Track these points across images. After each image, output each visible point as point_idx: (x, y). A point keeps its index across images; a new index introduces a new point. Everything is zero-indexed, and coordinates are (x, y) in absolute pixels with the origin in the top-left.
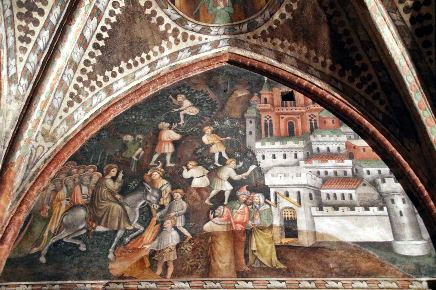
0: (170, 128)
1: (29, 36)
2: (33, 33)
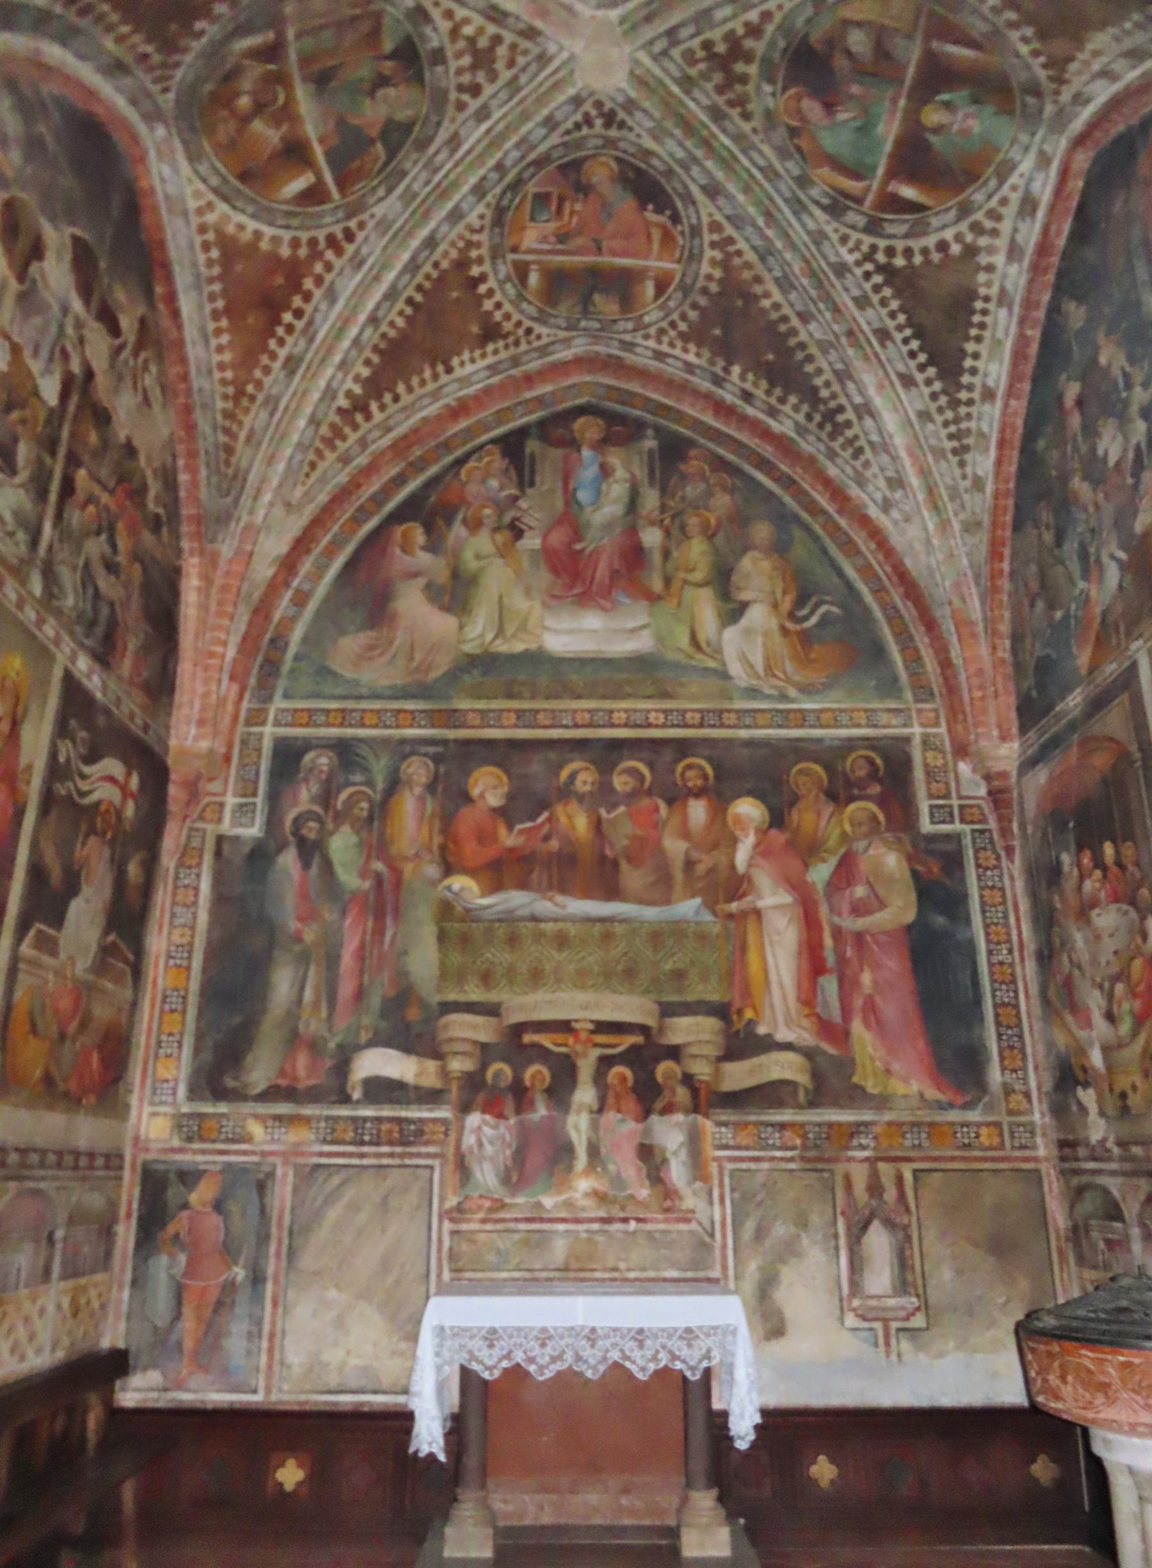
0: (1069, 379)
1: (857, 444)
2: (856, 437)
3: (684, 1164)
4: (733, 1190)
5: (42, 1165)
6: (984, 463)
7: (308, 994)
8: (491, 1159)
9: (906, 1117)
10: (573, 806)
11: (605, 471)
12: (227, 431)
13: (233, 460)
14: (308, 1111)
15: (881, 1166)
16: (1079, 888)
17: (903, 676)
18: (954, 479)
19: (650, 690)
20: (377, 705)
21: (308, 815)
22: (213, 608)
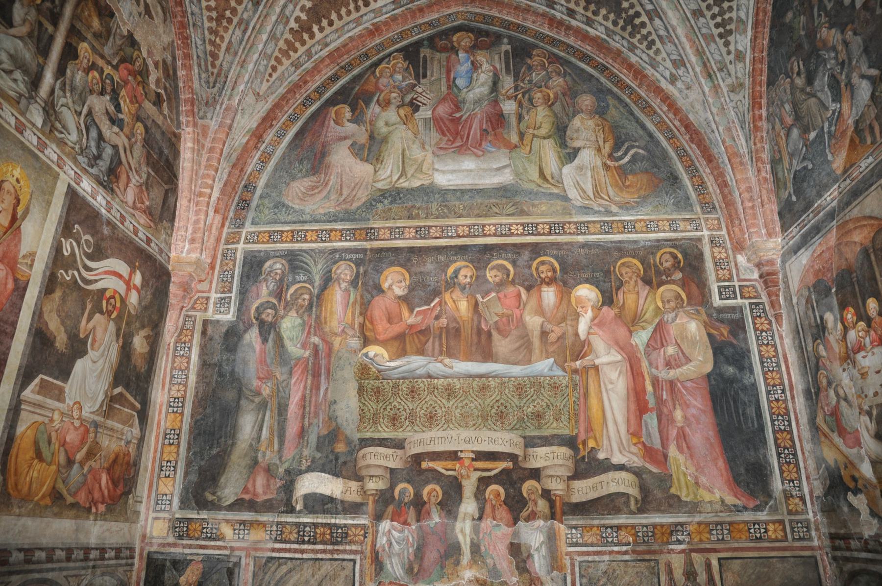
1: (649, 39)
2: (649, 33)
3: (544, 557)
4: (581, 576)
5: (50, 560)
6: (743, 41)
7: (265, 432)
8: (399, 555)
9: (710, 518)
10: (457, 294)
11: (475, 66)
12: (213, 43)
13: (218, 63)
14: (265, 518)
15: (693, 555)
16: (845, 337)
17: (693, 195)
18: (721, 55)
19: (512, 210)
20: (316, 227)
21: (267, 305)
22: (204, 163)
